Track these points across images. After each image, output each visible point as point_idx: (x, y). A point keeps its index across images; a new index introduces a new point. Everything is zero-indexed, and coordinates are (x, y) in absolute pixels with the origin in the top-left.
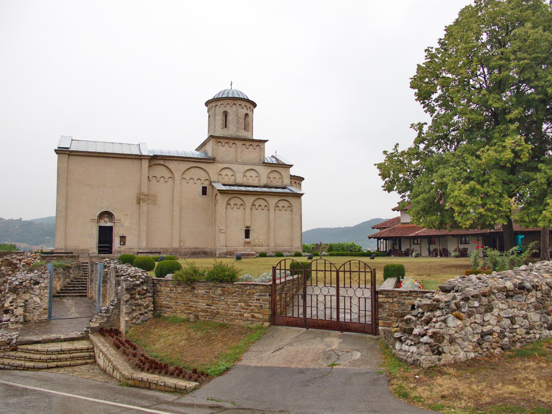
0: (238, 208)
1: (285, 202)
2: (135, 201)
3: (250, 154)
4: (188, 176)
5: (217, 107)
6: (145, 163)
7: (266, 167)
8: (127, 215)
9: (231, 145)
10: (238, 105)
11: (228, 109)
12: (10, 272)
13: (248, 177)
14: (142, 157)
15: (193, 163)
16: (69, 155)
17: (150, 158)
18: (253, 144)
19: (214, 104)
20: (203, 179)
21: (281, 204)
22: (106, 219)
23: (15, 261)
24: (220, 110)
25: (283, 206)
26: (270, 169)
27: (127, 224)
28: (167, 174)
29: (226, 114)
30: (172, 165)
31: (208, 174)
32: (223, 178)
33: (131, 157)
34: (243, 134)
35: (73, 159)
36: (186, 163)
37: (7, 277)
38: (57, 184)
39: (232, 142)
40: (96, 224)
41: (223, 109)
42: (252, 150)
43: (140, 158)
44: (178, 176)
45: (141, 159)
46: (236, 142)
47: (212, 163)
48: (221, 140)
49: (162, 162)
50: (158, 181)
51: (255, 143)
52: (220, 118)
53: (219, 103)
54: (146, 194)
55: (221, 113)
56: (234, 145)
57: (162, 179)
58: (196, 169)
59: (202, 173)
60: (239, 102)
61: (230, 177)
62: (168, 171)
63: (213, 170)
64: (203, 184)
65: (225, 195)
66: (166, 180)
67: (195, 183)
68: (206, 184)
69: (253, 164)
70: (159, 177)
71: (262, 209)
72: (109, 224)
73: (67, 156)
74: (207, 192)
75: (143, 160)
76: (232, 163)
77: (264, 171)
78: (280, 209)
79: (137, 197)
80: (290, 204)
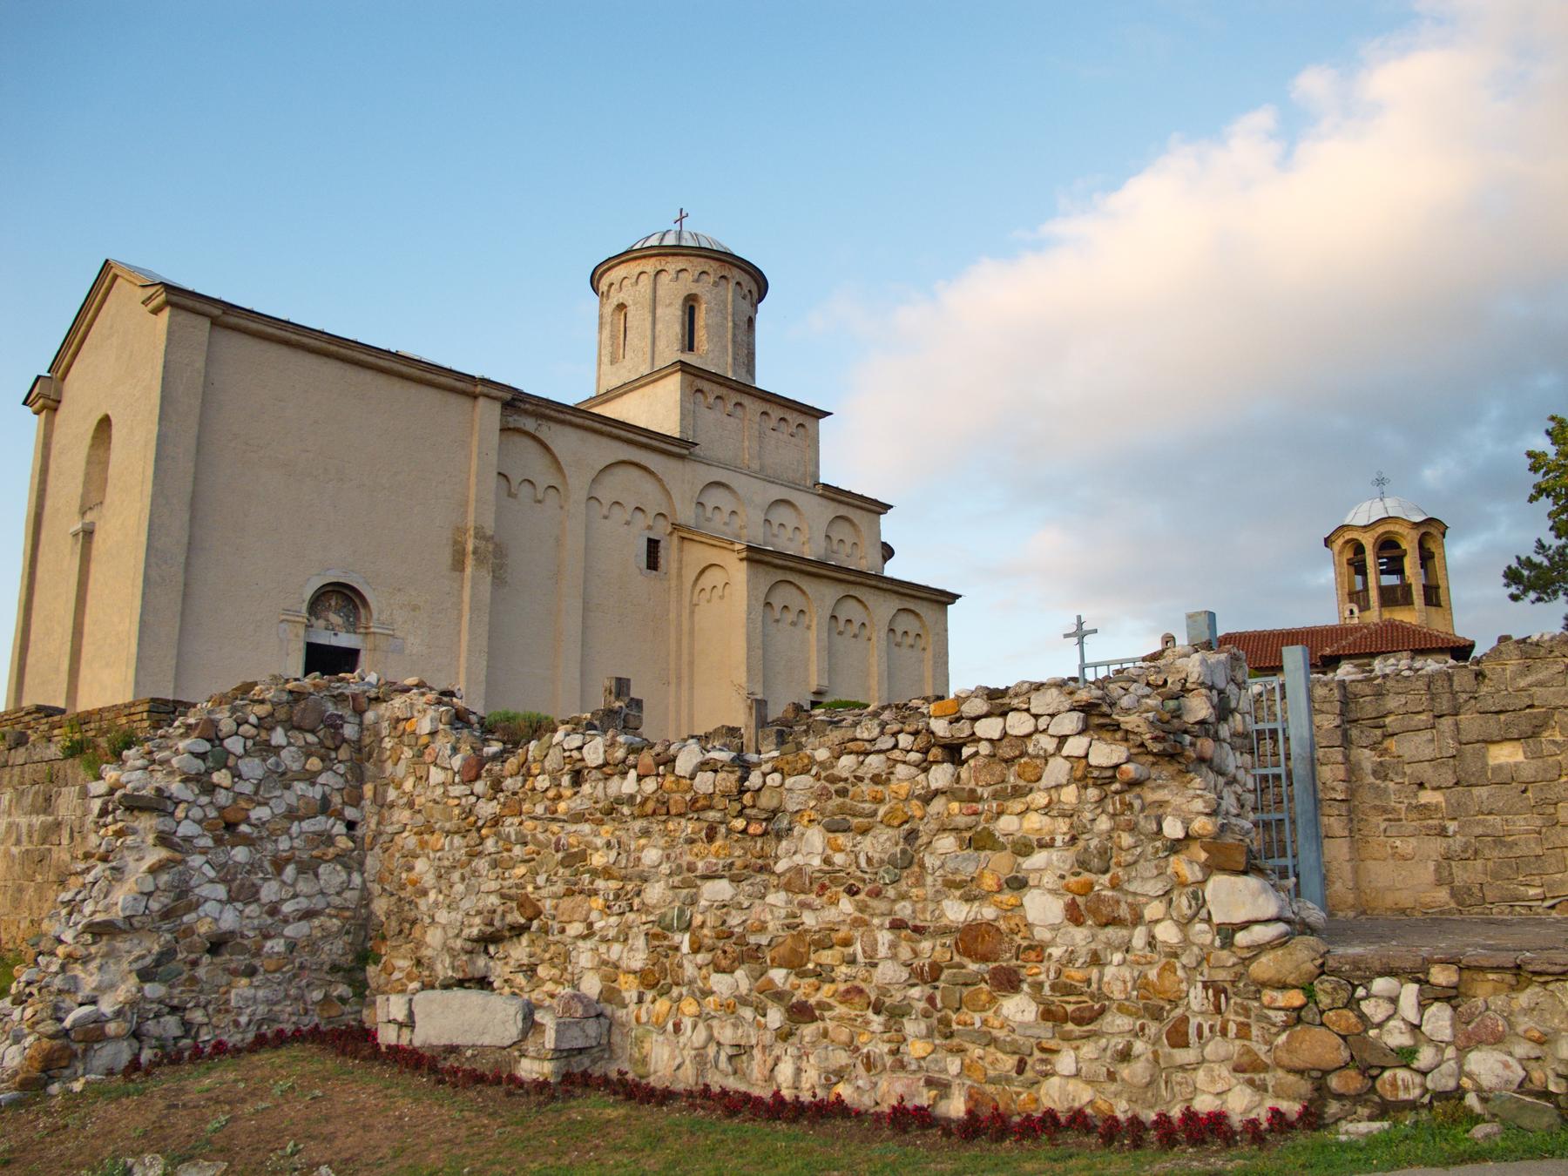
0: (794, 624)
1: (911, 617)
2: (446, 557)
3: (781, 451)
4: (607, 493)
5: (664, 278)
6: (488, 414)
7: (825, 502)
8: (415, 608)
9: (730, 407)
10: (731, 285)
11: (704, 290)
12: (314, 763)
13: (775, 523)
14: (479, 389)
15: (625, 447)
16: (215, 322)
17: (508, 396)
18: (788, 417)
19: (650, 266)
20: (651, 513)
21: (906, 622)
22: (335, 619)
23: (331, 709)
24: (672, 290)
25: (906, 633)
26: (832, 510)
27: (415, 644)
28: (544, 476)
29: (690, 306)
30: (564, 441)
31: (667, 493)
32: (709, 520)
33: (442, 380)
34: (744, 379)
35: (237, 348)
36: (605, 441)
37: (299, 787)
38: (159, 436)
39: (736, 397)
40: (302, 632)
41: (687, 285)
42: (786, 437)
43: (467, 387)
44: (578, 484)
45: (475, 397)
46: (746, 401)
47: (681, 457)
48: (706, 386)
49: (529, 424)
50: (510, 495)
51: (795, 414)
52: (671, 316)
53: (673, 264)
54: (489, 533)
55: (680, 301)
56: (739, 410)
57: (526, 488)
58: (635, 473)
59: (647, 485)
60: (737, 275)
61: (725, 516)
62: (547, 460)
63: (682, 479)
64: (650, 528)
65: (761, 569)
66: (540, 497)
67: (628, 523)
68: (661, 530)
69: (794, 485)
70: (515, 481)
71: (855, 636)
72: (344, 640)
73: (207, 323)
74: (662, 561)
75: (481, 401)
76: (736, 469)
77: (819, 513)
78: (899, 639)
79: (455, 543)
80: (923, 626)
